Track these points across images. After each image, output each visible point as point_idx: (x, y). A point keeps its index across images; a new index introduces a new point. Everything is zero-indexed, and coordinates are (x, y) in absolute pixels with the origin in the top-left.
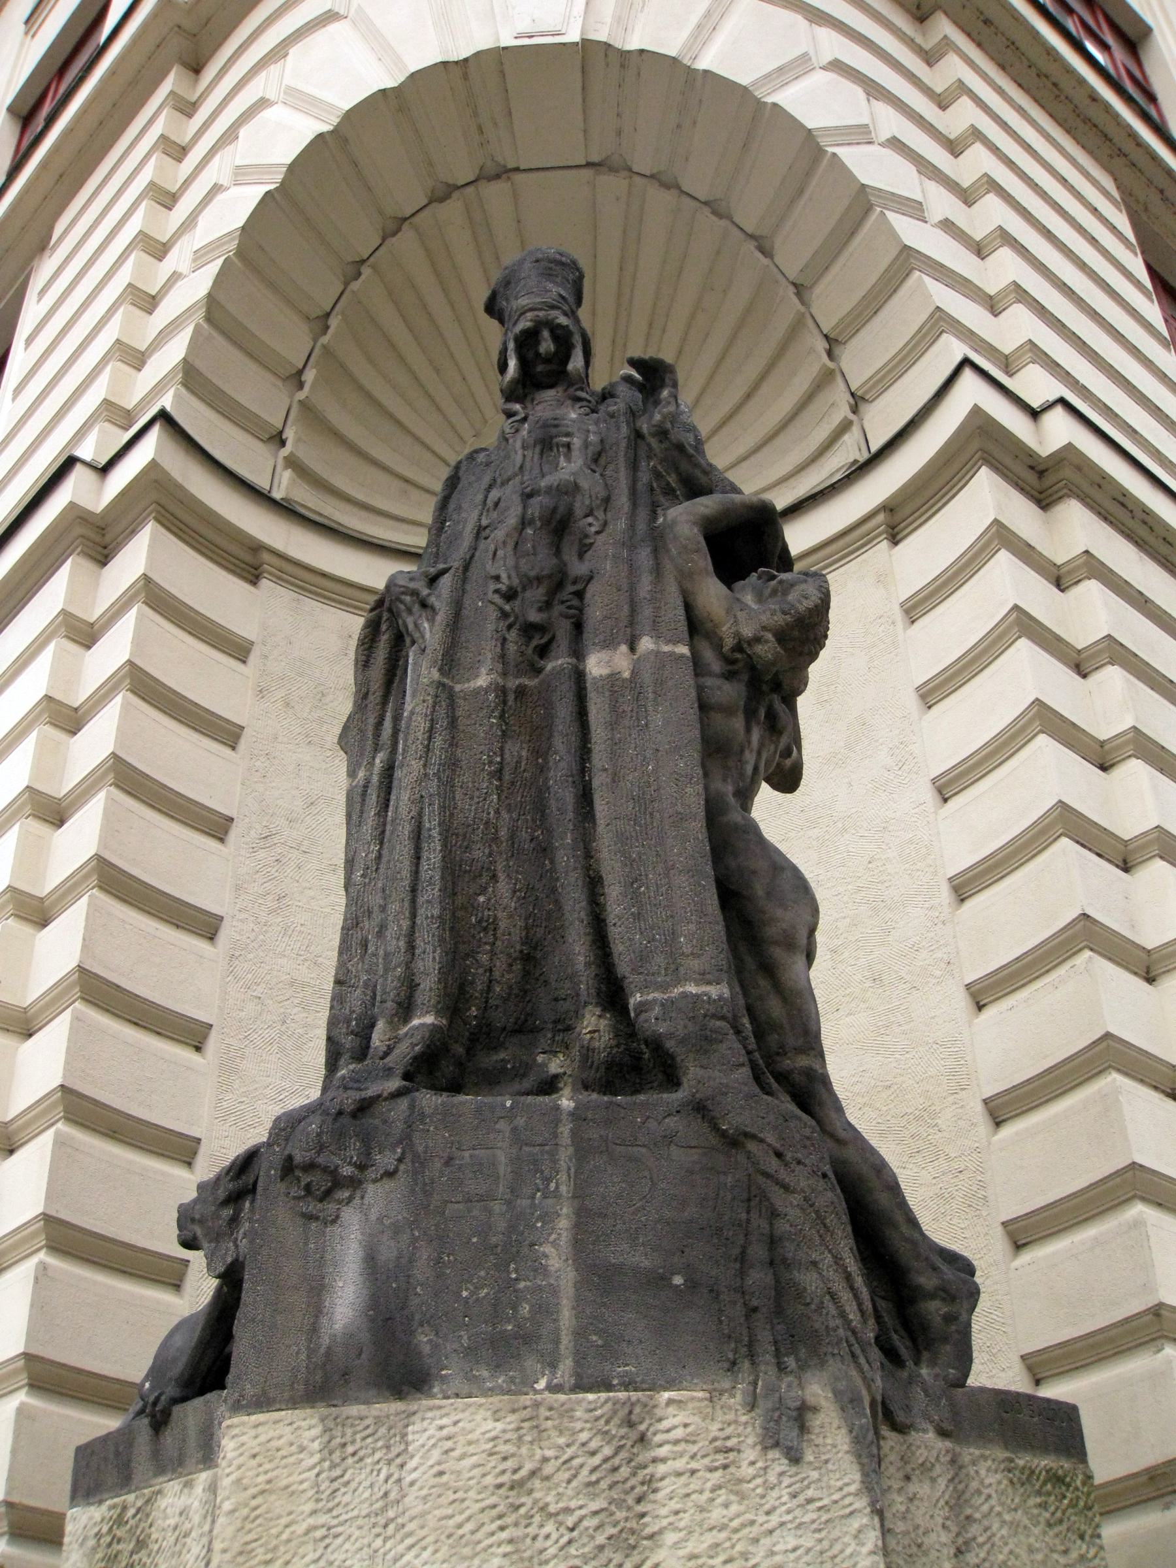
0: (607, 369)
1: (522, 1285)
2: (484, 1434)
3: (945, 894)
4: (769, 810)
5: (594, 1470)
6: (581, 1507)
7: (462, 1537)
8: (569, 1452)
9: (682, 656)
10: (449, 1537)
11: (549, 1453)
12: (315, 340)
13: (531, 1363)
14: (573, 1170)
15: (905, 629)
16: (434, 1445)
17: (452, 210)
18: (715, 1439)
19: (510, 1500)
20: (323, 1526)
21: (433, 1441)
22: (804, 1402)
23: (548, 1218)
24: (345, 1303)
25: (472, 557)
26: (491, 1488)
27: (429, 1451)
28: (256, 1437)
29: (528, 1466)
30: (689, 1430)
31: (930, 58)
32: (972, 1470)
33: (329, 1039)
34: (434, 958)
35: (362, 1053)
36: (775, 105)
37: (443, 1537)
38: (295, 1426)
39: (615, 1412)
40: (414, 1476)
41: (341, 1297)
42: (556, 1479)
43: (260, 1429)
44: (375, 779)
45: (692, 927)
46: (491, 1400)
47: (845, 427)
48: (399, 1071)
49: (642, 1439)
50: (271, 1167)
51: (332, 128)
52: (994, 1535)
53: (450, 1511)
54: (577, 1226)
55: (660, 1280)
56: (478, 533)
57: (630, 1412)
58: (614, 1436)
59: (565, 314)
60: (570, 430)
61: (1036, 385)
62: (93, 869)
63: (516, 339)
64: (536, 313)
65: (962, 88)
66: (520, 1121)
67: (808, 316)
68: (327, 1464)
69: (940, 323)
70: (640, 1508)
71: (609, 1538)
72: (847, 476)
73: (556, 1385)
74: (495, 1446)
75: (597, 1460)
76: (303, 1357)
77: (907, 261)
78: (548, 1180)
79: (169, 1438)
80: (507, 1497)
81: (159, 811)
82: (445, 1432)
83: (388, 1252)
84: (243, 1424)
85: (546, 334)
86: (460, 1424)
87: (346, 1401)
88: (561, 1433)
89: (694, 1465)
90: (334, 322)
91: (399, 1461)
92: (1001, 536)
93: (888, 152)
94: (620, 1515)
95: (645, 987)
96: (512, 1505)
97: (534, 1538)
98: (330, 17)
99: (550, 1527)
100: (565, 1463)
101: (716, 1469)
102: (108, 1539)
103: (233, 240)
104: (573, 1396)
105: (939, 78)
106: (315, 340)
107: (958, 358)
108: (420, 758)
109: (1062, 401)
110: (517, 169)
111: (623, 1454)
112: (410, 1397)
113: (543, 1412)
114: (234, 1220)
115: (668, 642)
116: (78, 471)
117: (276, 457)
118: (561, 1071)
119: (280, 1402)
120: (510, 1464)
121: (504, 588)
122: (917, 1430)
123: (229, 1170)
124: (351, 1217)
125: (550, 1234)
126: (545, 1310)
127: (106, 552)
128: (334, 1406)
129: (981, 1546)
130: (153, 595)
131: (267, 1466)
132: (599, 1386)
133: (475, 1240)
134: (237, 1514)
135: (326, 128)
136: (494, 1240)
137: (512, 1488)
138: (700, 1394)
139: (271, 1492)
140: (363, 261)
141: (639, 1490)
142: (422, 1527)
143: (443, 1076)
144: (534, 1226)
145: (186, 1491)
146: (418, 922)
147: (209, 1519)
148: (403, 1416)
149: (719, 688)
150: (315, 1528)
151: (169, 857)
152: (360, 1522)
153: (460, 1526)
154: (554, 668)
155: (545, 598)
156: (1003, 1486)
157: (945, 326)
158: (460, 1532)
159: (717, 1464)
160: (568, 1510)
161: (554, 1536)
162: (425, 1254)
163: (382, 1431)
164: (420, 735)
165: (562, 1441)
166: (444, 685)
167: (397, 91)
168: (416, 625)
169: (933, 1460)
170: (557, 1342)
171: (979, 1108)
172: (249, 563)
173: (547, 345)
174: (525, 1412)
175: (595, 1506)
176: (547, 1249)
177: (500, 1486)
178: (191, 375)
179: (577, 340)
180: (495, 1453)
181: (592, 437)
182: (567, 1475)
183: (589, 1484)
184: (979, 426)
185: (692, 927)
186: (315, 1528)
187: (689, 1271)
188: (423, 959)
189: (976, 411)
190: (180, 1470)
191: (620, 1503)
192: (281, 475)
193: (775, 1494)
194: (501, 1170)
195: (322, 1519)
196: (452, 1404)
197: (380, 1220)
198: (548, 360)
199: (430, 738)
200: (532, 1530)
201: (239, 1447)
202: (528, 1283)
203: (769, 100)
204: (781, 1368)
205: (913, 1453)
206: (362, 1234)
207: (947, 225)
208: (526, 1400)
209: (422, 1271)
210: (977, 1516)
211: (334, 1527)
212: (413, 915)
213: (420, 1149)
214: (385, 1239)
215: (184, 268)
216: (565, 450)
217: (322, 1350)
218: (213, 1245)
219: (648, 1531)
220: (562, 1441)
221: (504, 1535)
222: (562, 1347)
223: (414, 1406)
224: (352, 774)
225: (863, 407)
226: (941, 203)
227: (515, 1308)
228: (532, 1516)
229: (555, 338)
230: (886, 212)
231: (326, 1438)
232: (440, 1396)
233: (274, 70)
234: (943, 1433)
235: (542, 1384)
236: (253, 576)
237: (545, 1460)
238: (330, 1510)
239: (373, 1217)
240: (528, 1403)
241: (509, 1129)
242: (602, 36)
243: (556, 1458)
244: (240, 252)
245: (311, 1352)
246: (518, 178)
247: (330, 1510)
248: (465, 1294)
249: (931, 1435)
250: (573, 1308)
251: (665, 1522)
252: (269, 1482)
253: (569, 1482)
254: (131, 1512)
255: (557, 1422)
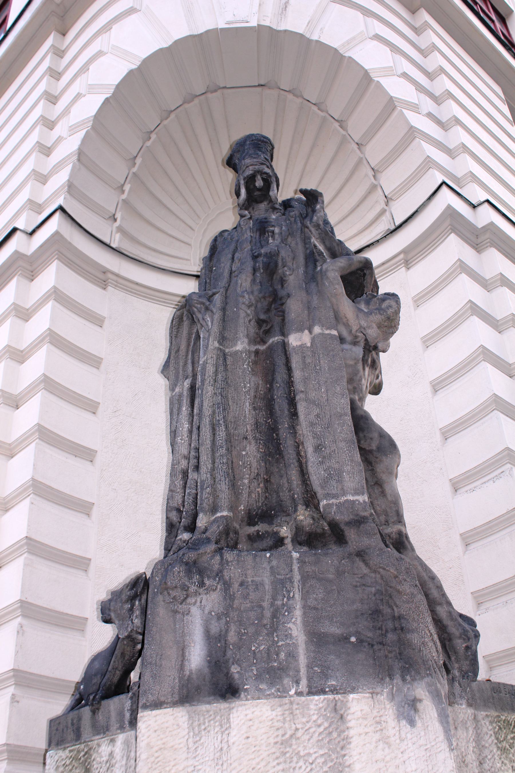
0: (285, 192)
1: (280, 643)
2: (267, 717)
3: (438, 437)
4: (371, 405)
5: (320, 734)
6: (315, 753)
7: (260, 768)
8: (308, 725)
9: (335, 335)
10: (253, 769)
11: (299, 726)
12: (129, 170)
13: (287, 681)
14: (300, 586)
15: (415, 310)
16: (244, 723)
17: (193, 107)
18: (376, 717)
19: (282, 750)
20: (192, 765)
21: (243, 721)
22: (415, 698)
23: (290, 610)
25: (229, 286)
26: (272, 744)
27: (241, 726)
28: (156, 721)
29: (289, 733)
30: (364, 712)
31: (417, 31)
32: (483, 722)
33: (167, 518)
34: (226, 483)
35: (191, 528)
36: (350, 57)
37: (250, 769)
38: (175, 715)
39: (328, 705)
40: (235, 739)
41: (193, 651)
42: (303, 738)
43: (158, 717)
44: (185, 393)
45: (349, 467)
46: (269, 700)
47: (383, 212)
48: (214, 540)
49: (342, 717)
50: (155, 588)
51: (136, 67)
52: (494, 754)
53: (252, 756)
54: (304, 613)
55: (346, 639)
56: (231, 273)
57: (336, 705)
58: (329, 717)
59: (268, 167)
60: (273, 224)
61: (477, 195)
62: (36, 430)
63: (244, 179)
64: (254, 167)
65: (434, 47)
66: (274, 563)
67: (364, 159)
68: (191, 734)
69: (429, 163)
70: (343, 752)
71: (329, 768)
72: (385, 237)
73: (300, 692)
74: (273, 723)
75: (322, 729)
76: (177, 681)
77: (412, 133)
78: (289, 592)
79: (100, 717)
80: (280, 748)
81: (65, 400)
82: (249, 717)
83: (215, 628)
84: (149, 715)
85: (259, 177)
86: (255, 713)
87: (199, 702)
88: (303, 716)
89: (366, 730)
90: (138, 161)
91: (227, 732)
92: (462, 267)
93: (402, 80)
94: (333, 756)
95: (328, 496)
96: (282, 752)
97: (294, 768)
98: (132, 11)
99: (301, 763)
100: (306, 730)
101: (377, 731)
102: (70, 767)
103: (90, 121)
104: (308, 698)
105: (423, 41)
106: (129, 170)
107: (440, 182)
108: (212, 385)
109: (488, 201)
110: (225, 88)
111: (334, 726)
112: (230, 700)
113: (295, 706)
114: (131, 610)
115: (327, 329)
116: (18, 237)
117: (112, 227)
118: (285, 535)
119: (167, 703)
120: (280, 732)
121: (247, 303)
122: (458, 704)
123: (127, 586)
124: (195, 611)
125: (292, 618)
126: (292, 655)
127: (32, 274)
128: (194, 705)
129: (489, 760)
130: (57, 295)
131: (162, 736)
132: (320, 692)
133: (256, 622)
134: (149, 760)
135: (134, 67)
136: (265, 622)
137: (282, 744)
138: (367, 695)
139: (165, 749)
140: (152, 132)
141: (342, 743)
142: (240, 764)
143: (232, 539)
144: (284, 615)
145: (111, 743)
146: (216, 465)
147: (125, 758)
148: (227, 710)
149: (351, 350)
150: (188, 766)
151: (72, 423)
152: (209, 763)
153: (258, 764)
154: (273, 342)
155: (267, 307)
156: (496, 730)
157: (431, 165)
158: (259, 767)
159: (378, 729)
160: (309, 754)
161: (304, 767)
163: (218, 718)
164: (211, 374)
165: (304, 720)
166: (220, 349)
167: (169, 49)
168: (203, 319)
169: (466, 719)
170: (298, 671)
171: (458, 537)
172: (102, 278)
173: (259, 183)
174: (286, 706)
175: (321, 752)
176: (290, 625)
177: (276, 743)
178: (71, 187)
179: (273, 179)
180: (273, 727)
181: (284, 228)
182: (308, 737)
183: (318, 741)
184: (450, 213)
185: (349, 467)
186: (188, 766)
187: (357, 634)
188: (220, 484)
189: (449, 207)
190: (107, 733)
191: (334, 751)
192: (115, 236)
193: (405, 742)
194: (267, 587)
195: (191, 762)
196: (251, 703)
197: (210, 613)
198: (259, 190)
199: (216, 376)
200: (293, 765)
201: (147, 728)
202: (283, 643)
203: (347, 55)
204: (404, 680)
205: (458, 717)
206: (202, 620)
207: (430, 115)
208: (286, 700)
209: (232, 637)
210: (487, 745)
211: (197, 766)
212: (214, 462)
213: (227, 578)
214: (213, 622)
215: (64, 134)
216: (272, 234)
217: (186, 678)
218: (121, 622)
219: (347, 763)
220: (304, 720)
221: (280, 767)
222: (301, 673)
223: (233, 705)
224: (172, 389)
225: (391, 203)
226: (428, 105)
227: (277, 655)
228: (292, 758)
229: (263, 179)
230: (403, 110)
231: (191, 722)
232: (244, 699)
233: (104, 37)
234: (470, 705)
235: (292, 692)
236: (104, 284)
237: (297, 729)
238: (195, 757)
239: (206, 612)
240: (287, 701)
241: (268, 568)
242: (267, 23)
243: (302, 728)
244: (93, 127)
245: (181, 679)
246: (226, 91)
247: (195, 757)
248: (253, 648)
249: (464, 706)
250: (305, 654)
251: (355, 758)
252: (164, 744)
253: (309, 740)
254: (82, 753)
255: (301, 711)
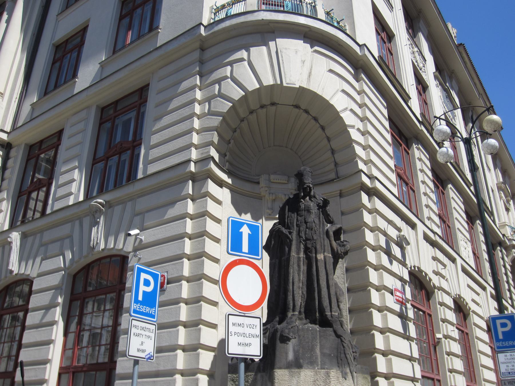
23: (316, 346)
24: (291, 356)
49: (329, 376)
55: (330, 355)
83: (296, 348)
126: (317, 358)
162: (301, 350)
209: (301, 351)
226: (359, 125)
